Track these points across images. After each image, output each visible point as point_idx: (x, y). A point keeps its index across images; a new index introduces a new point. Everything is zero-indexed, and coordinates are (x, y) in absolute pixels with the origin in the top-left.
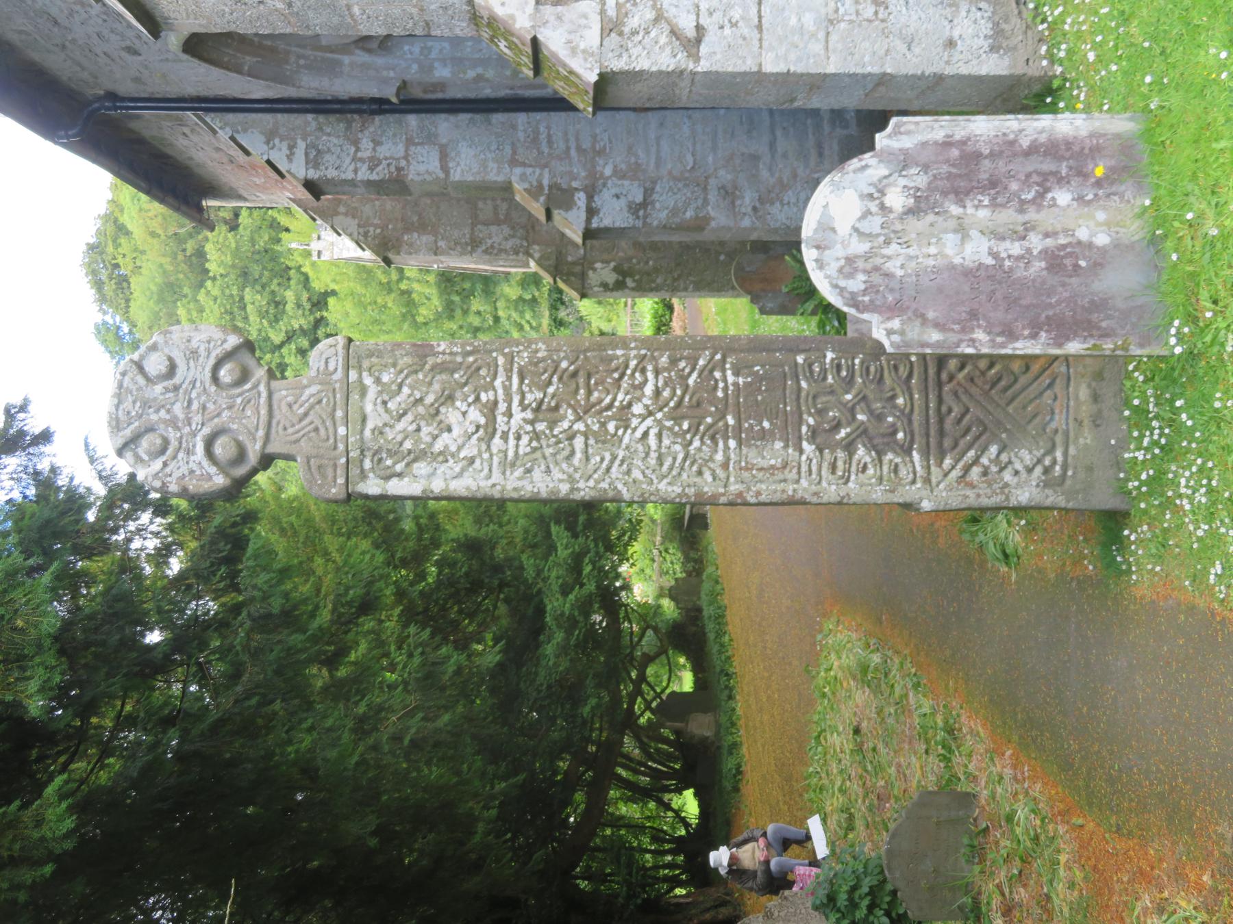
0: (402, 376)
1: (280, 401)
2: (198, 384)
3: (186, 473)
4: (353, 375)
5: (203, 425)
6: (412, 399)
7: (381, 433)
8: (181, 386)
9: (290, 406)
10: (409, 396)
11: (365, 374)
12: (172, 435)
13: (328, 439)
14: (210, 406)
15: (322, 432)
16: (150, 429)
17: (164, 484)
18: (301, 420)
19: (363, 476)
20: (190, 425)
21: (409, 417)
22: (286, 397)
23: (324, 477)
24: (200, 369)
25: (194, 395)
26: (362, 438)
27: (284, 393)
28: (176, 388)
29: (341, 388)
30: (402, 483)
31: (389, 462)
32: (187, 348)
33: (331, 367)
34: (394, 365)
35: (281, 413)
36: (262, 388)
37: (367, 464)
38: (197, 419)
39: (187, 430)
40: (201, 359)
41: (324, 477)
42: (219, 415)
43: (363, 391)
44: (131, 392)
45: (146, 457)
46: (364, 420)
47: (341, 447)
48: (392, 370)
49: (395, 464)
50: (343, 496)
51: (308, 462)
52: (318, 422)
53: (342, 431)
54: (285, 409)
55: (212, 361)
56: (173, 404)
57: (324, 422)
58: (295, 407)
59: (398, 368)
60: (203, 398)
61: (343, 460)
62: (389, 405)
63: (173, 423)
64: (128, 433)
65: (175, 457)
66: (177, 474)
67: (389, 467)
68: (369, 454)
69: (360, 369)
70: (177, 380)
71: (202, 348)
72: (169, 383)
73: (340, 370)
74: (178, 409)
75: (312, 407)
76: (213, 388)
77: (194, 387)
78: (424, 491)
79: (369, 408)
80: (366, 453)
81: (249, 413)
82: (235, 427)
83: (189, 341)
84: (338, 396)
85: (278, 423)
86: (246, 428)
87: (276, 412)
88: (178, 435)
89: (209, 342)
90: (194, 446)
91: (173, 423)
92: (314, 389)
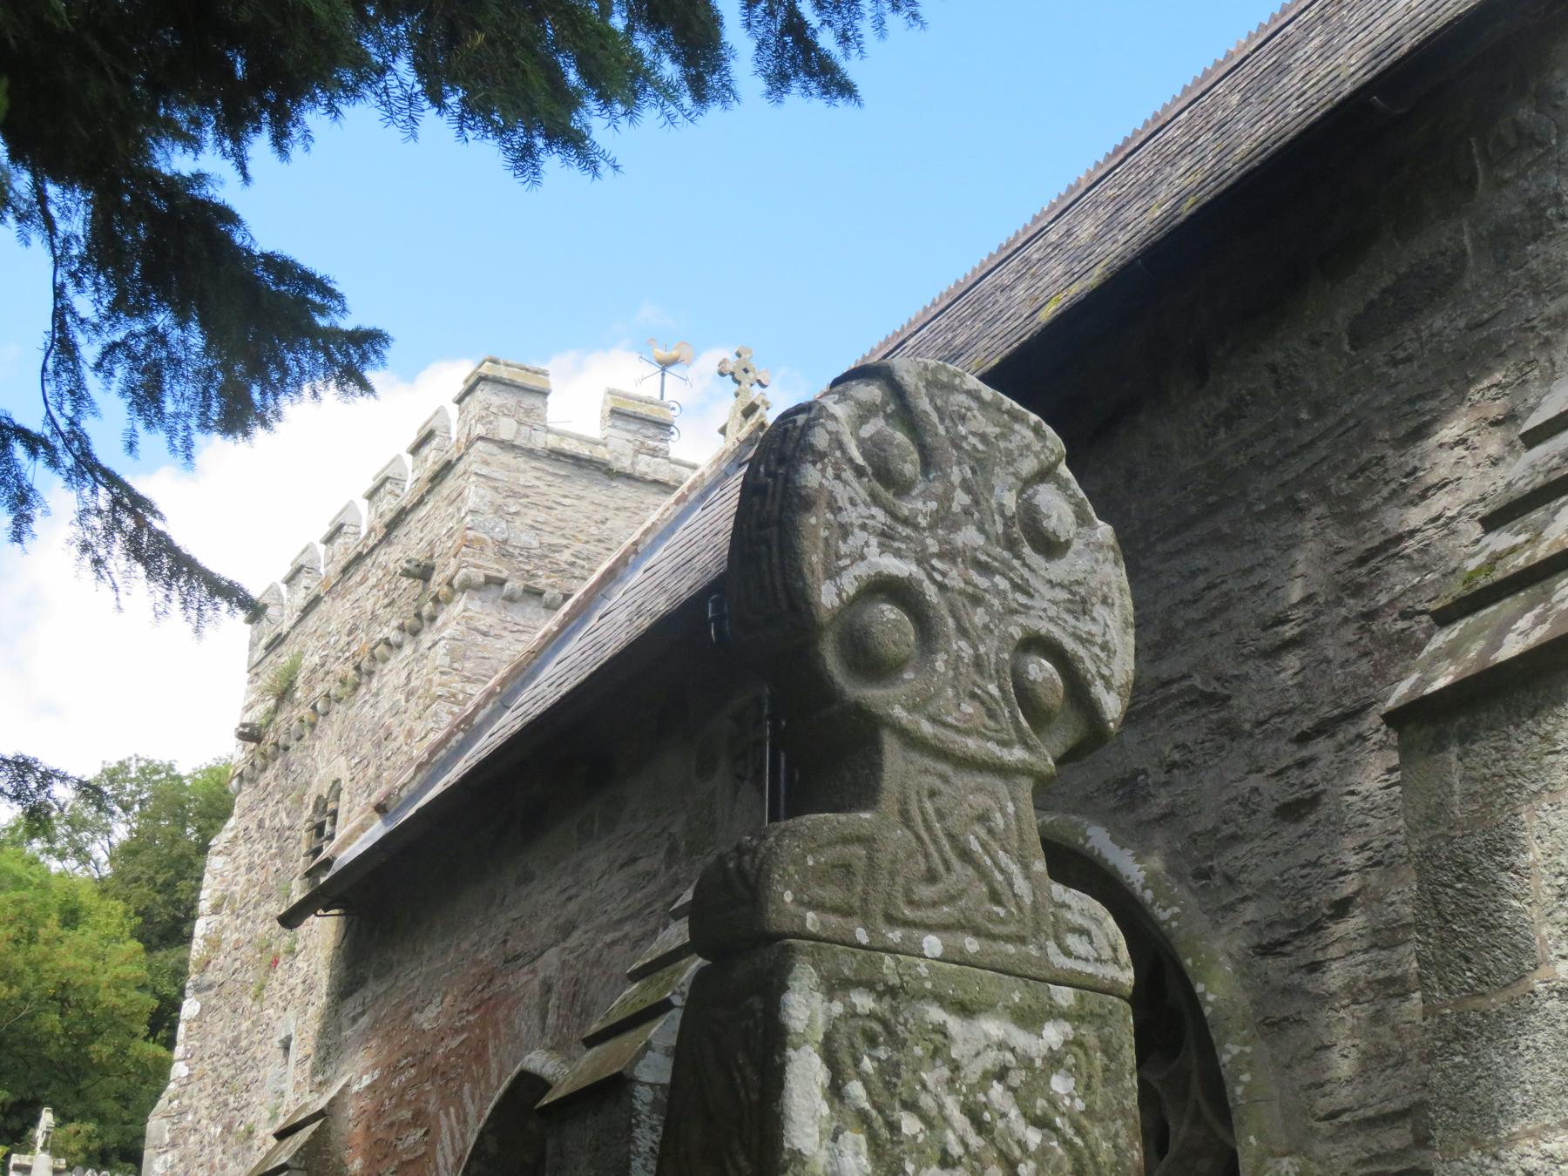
0: (1070, 1132)
1: (993, 794)
2: (1022, 599)
3: (844, 518)
4: (1065, 996)
5: (942, 587)
6: (1017, 1153)
7: (936, 1052)
8: (1018, 556)
9: (983, 818)
10: (1022, 1145)
11: (1067, 1027)
12: (919, 506)
13: (911, 903)
14: (979, 617)
15: (925, 892)
16: (928, 460)
17: (822, 456)
18: (951, 837)
19: (835, 986)
20: (941, 556)
21: (975, 1141)
22: (1002, 810)
23: (822, 876)
24: (1053, 611)
25: (1003, 583)
26: (923, 996)
27: (1011, 808)
28: (1011, 544)
29: (1028, 958)
30: (818, 1092)
31: (867, 1065)
32: (1092, 592)
33: (1072, 941)
34: (1089, 1112)
35: (972, 793)
36: (1017, 754)
37: (864, 1002)
38: (955, 580)
39: (933, 547)
40: (1069, 618)
41: (822, 876)
42: (963, 632)
43: (1029, 1019)
44: (1002, 436)
45: (867, 431)
46: (965, 1010)
47: (895, 936)
48: (1080, 1105)
49: (866, 1081)
50: (776, 920)
51: (859, 840)
52: (949, 883)
53: (933, 944)
54: (980, 801)
55: (1070, 645)
56: (981, 530)
57: (951, 899)
58: (983, 833)
59: (1085, 1122)
60: (996, 602)
61: (862, 936)
62: (997, 1089)
63: (944, 520)
64: (924, 404)
65: (875, 499)
66: (842, 494)
67: (857, 1062)
68: (883, 1008)
69: (1075, 1017)
70: (1027, 550)
71: (1094, 629)
72: (1017, 531)
73: (1069, 963)
74: (968, 536)
75: (983, 874)
76: (1017, 633)
77: (1016, 587)
78: (798, 1156)
79: (993, 1027)
80: (887, 999)
81: (968, 708)
82: (940, 666)
83: (1105, 601)
84: (1011, 949)
85: (945, 779)
86: (937, 695)
87: (966, 780)
88: (923, 523)
89: (1105, 647)
90: (898, 554)
91: (944, 520)
92: (1021, 886)
